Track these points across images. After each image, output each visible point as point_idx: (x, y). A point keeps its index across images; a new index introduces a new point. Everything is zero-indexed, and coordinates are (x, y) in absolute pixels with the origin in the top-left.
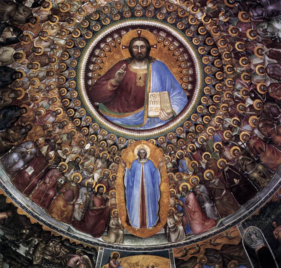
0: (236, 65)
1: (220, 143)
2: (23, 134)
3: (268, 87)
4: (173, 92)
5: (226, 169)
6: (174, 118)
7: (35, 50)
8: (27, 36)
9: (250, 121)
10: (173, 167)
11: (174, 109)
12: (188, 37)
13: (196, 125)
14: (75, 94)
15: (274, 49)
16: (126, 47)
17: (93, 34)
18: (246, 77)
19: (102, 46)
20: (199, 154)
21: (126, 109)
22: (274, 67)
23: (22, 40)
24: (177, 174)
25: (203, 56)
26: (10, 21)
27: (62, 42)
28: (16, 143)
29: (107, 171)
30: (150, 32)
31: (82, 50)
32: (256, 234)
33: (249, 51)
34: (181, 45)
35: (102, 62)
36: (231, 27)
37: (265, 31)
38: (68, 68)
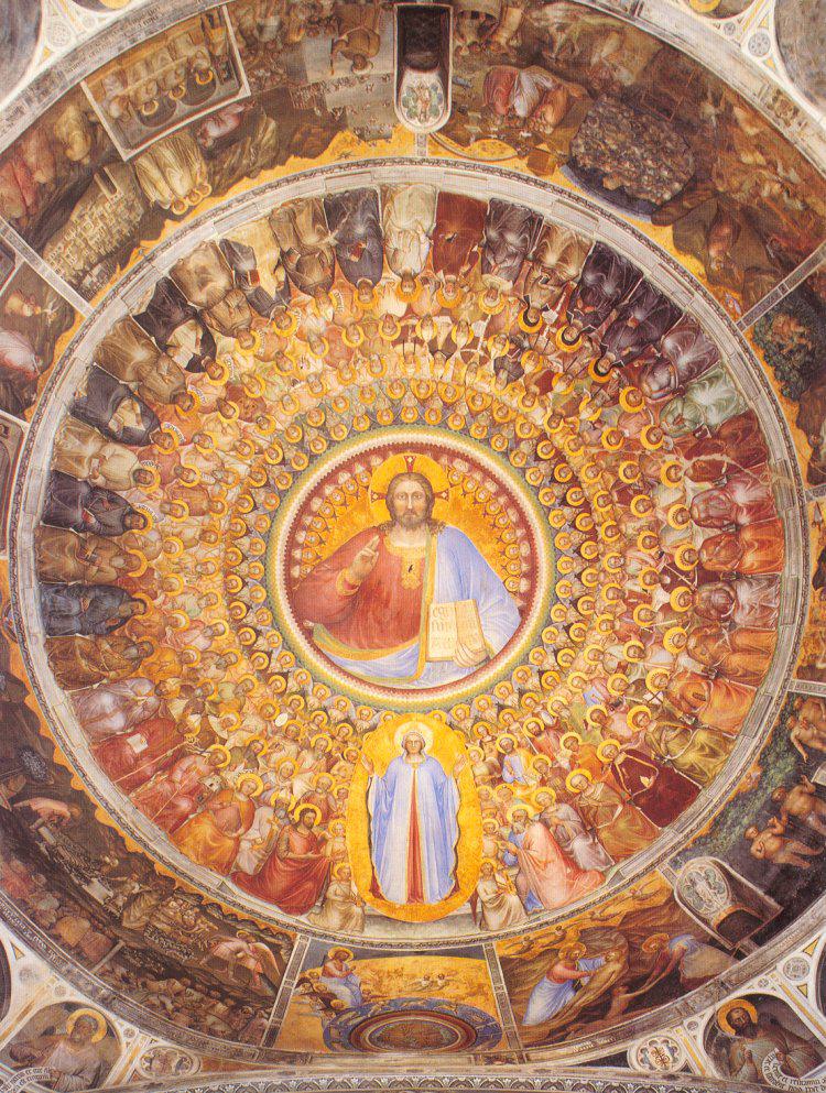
0: (625, 518)
1: (602, 707)
2: (132, 659)
3: (699, 552)
4: (487, 598)
5: (620, 759)
6: (488, 661)
7: (181, 472)
9: (666, 642)
10: (491, 774)
11: (488, 641)
13: (541, 673)
14: (261, 595)
15: (703, 458)
16: (381, 496)
17: (310, 462)
18: (648, 541)
19: (328, 490)
20: (552, 740)
21: (376, 641)
22: (706, 501)
24: (500, 786)
25: (549, 509)
27: (242, 469)
28: (112, 674)
29: (326, 778)
31: (282, 494)
32: (707, 878)
34: (503, 490)
35: (327, 529)
36: (606, 430)
37: (679, 420)
38: (248, 532)
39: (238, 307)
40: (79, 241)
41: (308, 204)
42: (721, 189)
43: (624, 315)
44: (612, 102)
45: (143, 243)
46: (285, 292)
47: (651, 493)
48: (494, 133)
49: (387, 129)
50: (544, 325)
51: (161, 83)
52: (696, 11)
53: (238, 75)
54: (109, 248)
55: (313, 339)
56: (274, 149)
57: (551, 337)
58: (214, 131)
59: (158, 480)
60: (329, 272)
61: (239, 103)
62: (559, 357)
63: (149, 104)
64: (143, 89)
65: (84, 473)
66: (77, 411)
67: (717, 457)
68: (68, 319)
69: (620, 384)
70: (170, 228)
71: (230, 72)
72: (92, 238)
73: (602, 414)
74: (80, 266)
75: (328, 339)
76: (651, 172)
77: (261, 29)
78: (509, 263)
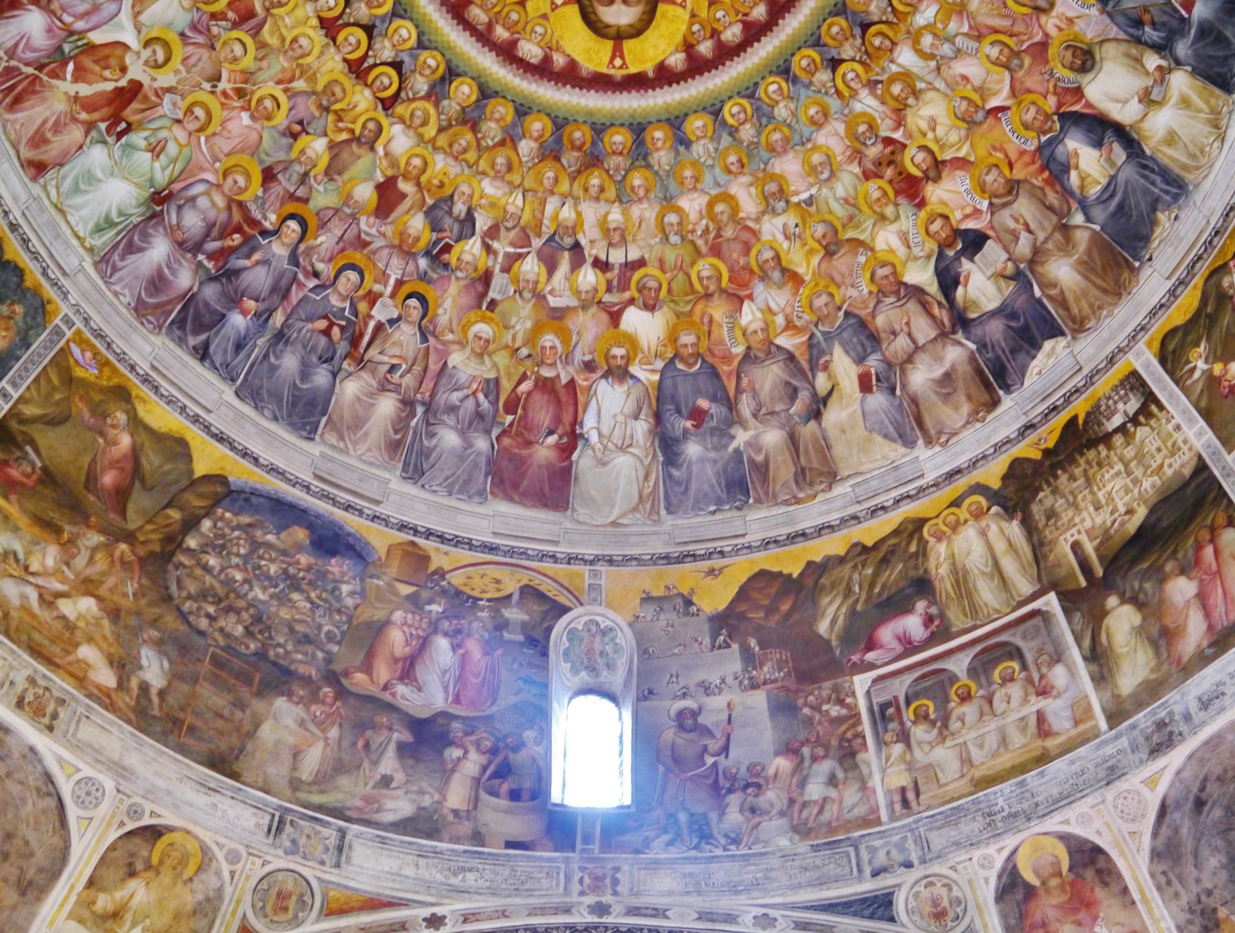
8: (1026, 127)
12: (436, 49)
15: (109, 86)
17: (787, 62)
23: (1048, 117)
26: (1069, 213)
27: (906, 57)
30: (578, 58)
33: (201, 39)
37: (156, 150)
39: (894, 334)
40: (1138, 472)
41: (775, 496)
42: (123, 546)
43: (263, 317)
44: (302, 669)
45: (1037, 455)
46: (816, 354)
47: (196, 16)
48: (482, 609)
49: (649, 612)
50: (393, 295)
51: (986, 708)
52: (188, 832)
53: (871, 710)
54: (1091, 454)
55: (776, 275)
56: (823, 589)
57: (383, 277)
58: (913, 624)
59: (1052, 51)
60: (745, 381)
61: (872, 666)
62: (366, 244)
63: (1008, 679)
64: (1015, 703)
65: (1180, 81)
66: (1175, 187)
67: (85, 90)
68: (1171, 347)
69: (262, 203)
70: (992, 474)
71: (884, 714)
72: (1118, 474)
73: (290, 147)
74: (1141, 433)
75: (752, 272)
76: (235, 560)
77: (832, 781)
78: (455, 397)
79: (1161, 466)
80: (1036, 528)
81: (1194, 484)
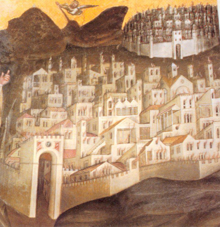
54: (118, 67)
72: (132, 111)
74: (182, 84)
79: (180, 139)
80: (16, 108)
81: (201, 192)
